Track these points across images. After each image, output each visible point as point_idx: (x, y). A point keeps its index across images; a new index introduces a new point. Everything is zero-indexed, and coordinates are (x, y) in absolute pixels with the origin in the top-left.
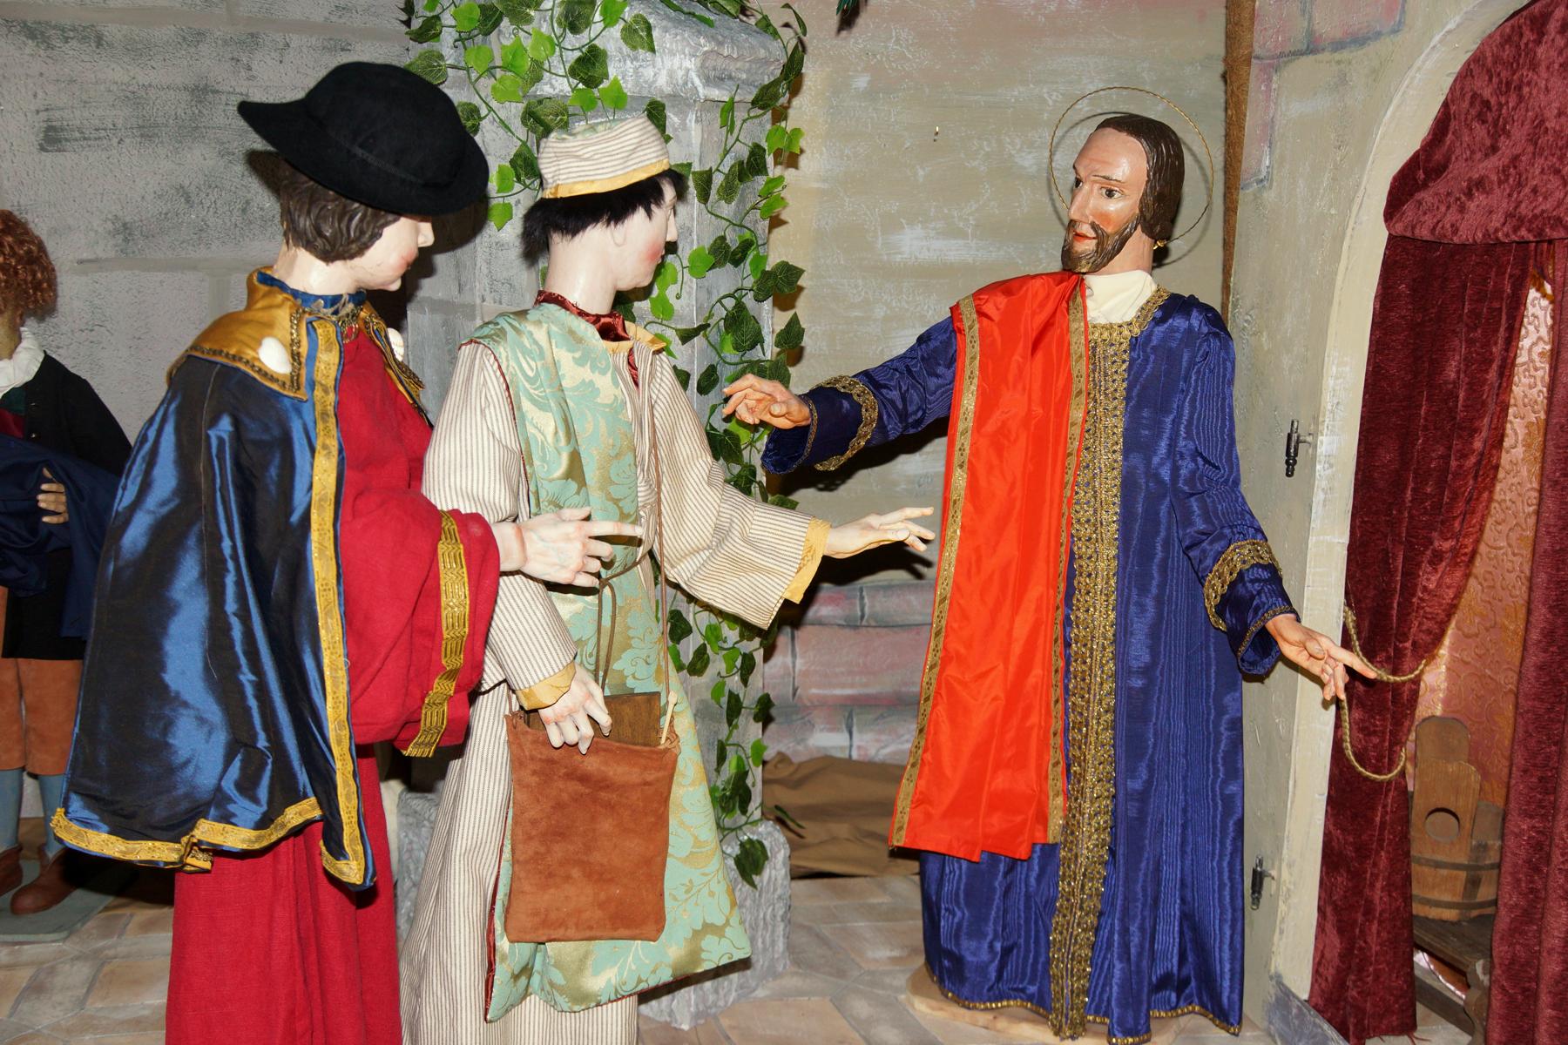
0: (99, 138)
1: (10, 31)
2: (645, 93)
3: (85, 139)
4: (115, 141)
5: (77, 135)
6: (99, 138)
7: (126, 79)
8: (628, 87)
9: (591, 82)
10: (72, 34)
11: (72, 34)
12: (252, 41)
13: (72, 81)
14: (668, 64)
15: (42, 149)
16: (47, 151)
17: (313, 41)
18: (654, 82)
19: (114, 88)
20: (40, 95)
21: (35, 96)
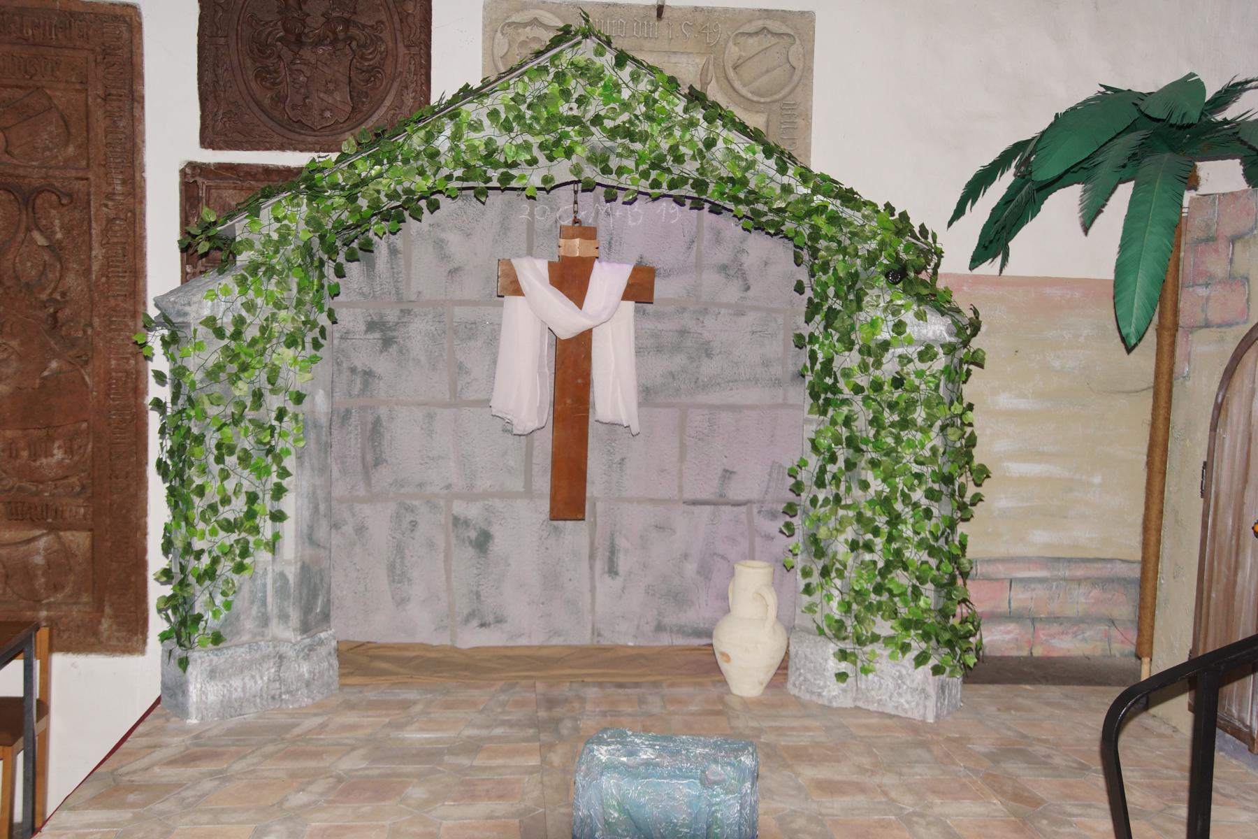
8: (915, 336)
9: (899, 334)
12: (705, 311)
17: (730, 311)
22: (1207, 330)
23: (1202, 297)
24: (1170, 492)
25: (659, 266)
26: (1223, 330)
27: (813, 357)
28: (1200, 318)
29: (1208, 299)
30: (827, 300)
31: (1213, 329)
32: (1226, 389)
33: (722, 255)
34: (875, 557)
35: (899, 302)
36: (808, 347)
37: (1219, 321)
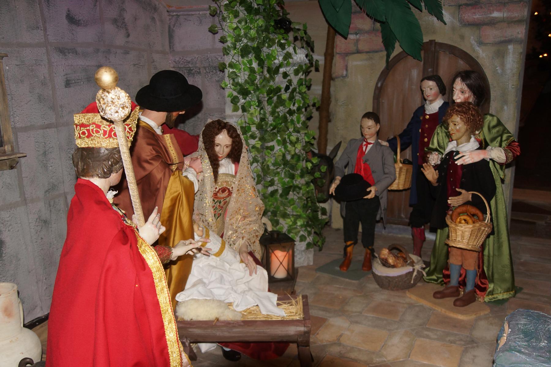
0: (78, 82)
1: (56, 51)
2: (295, 62)
3: (75, 83)
4: (82, 83)
5: (74, 81)
6: (78, 82)
7: (83, 64)
10: (70, 51)
11: (70, 51)
13: (72, 65)
14: (300, 56)
15: (66, 87)
16: (67, 87)
18: (297, 60)
19: (81, 67)
20: (65, 70)
21: (63, 70)
22: (359, 55)
23: (354, 40)
24: (338, 130)
25: (80, 18)
26: (371, 54)
27: (233, 77)
28: (353, 48)
29: (358, 41)
30: (241, 42)
31: (365, 54)
32: (384, 81)
33: (112, 12)
34: (276, 188)
35: (283, 41)
36: (226, 71)
37: (368, 50)
